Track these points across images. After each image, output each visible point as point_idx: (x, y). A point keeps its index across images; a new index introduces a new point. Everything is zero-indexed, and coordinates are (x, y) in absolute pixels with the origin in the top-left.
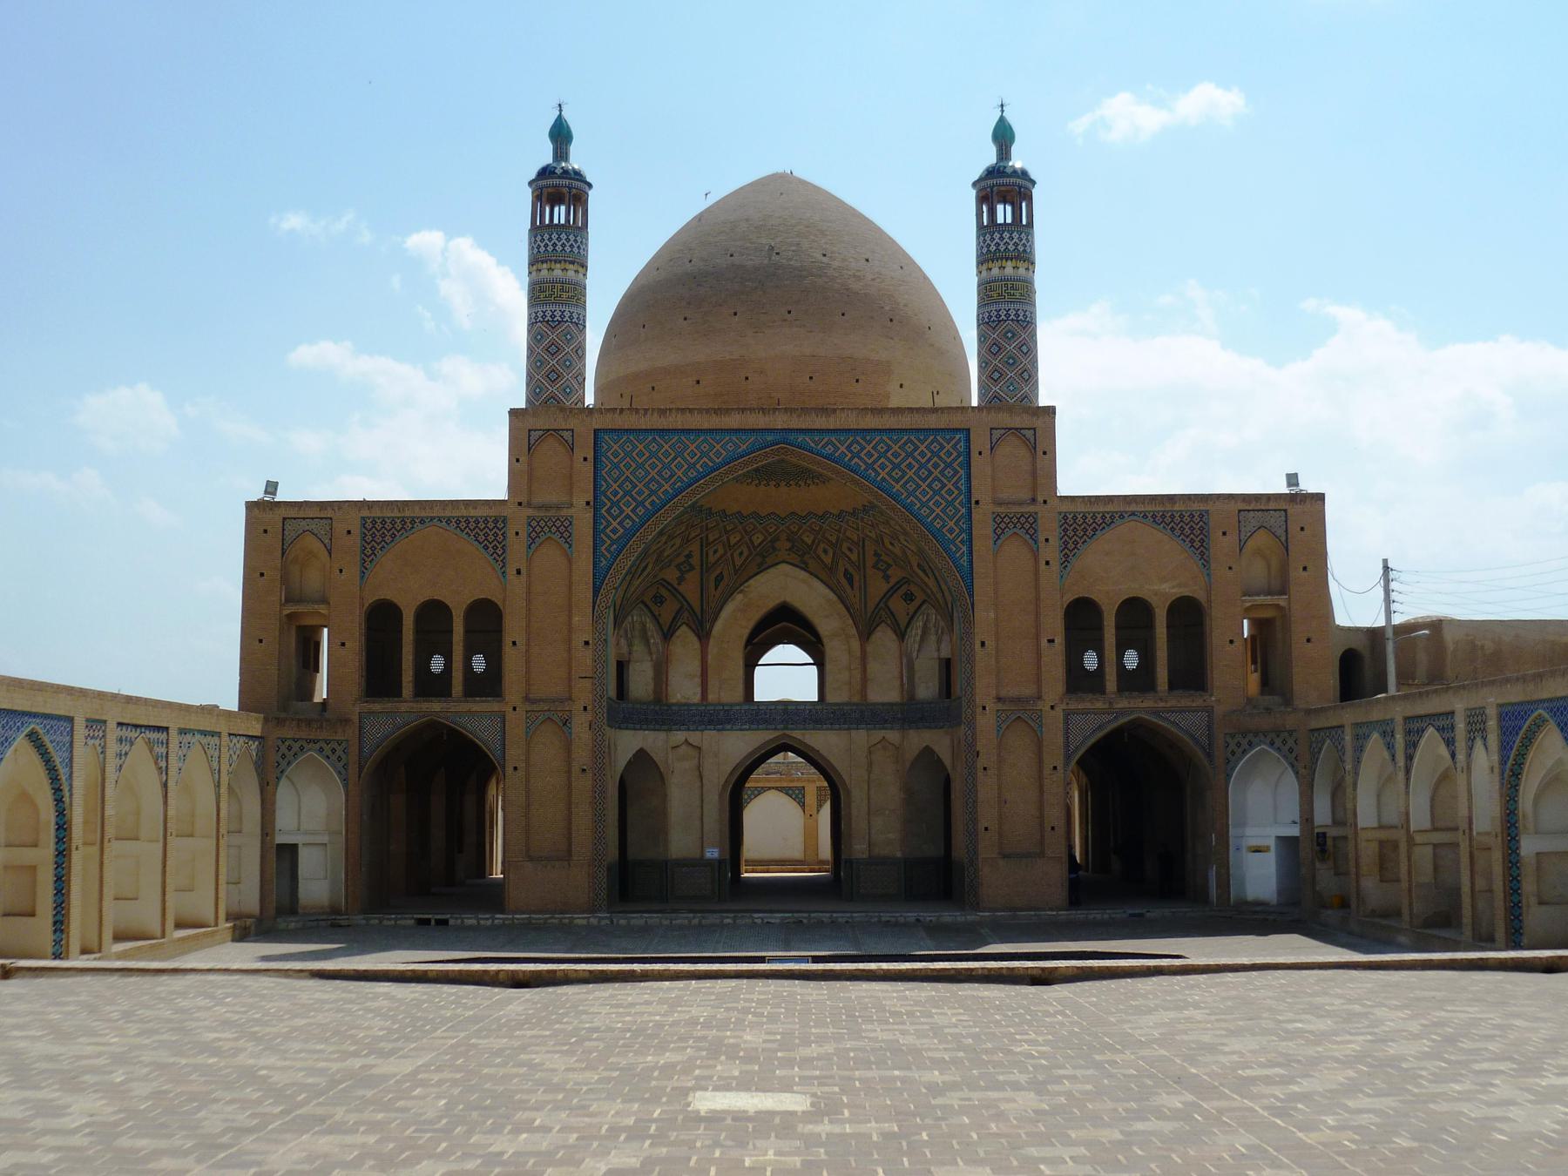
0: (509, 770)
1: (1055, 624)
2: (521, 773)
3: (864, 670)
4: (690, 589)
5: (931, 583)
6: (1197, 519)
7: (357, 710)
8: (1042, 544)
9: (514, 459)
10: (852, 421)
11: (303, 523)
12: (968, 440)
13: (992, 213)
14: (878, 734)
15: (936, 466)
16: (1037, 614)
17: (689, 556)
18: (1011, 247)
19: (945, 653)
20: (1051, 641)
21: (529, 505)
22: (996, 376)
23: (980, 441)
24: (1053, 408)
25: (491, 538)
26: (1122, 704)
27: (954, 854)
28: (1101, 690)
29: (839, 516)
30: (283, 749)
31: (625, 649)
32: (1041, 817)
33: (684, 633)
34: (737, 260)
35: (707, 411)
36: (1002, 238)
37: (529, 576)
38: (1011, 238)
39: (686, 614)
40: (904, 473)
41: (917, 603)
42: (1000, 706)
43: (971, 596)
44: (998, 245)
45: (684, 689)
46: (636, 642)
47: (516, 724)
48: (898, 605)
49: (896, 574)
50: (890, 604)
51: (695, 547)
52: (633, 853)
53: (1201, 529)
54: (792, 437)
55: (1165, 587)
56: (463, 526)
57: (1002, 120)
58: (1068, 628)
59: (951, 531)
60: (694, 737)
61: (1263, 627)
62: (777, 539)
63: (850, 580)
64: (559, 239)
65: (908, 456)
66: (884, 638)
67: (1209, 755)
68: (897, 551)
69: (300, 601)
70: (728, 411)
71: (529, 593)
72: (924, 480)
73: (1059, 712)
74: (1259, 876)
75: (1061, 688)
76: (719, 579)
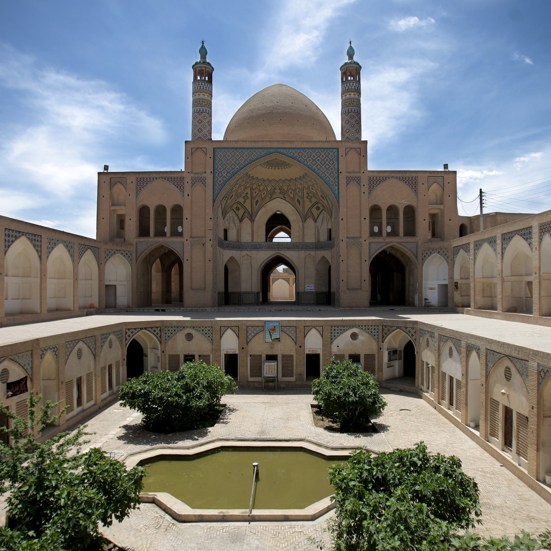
0: (185, 260)
1: (366, 213)
2: (189, 261)
3: (304, 232)
4: (248, 205)
5: (325, 202)
6: (414, 179)
7: (135, 241)
8: (362, 186)
9: (187, 158)
10: (299, 145)
11: (117, 179)
12: (338, 152)
13: (347, 79)
14: (308, 252)
15: (327, 160)
16: (360, 211)
17: (247, 194)
18: (353, 88)
19: (329, 227)
20: (365, 219)
21: (192, 173)
22: (348, 131)
23: (342, 152)
24: (367, 141)
25: (179, 184)
26: (388, 240)
27: (332, 290)
28: (382, 236)
29: (295, 180)
30: (107, 252)
31: (228, 225)
32: (361, 277)
33: (246, 221)
34: (264, 104)
35: (251, 141)
36: (350, 85)
37: (192, 196)
38: (353, 85)
39: (247, 214)
40: (317, 163)
41: (320, 210)
42: (348, 240)
43: (339, 203)
44: (348, 87)
45: (246, 238)
46: (231, 223)
47: (187, 245)
48: (314, 210)
49: (314, 200)
50: (312, 210)
51: (248, 190)
52: (230, 290)
53: (415, 182)
54: (279, 150)
55: (403, 201)
56: (170, 179)
57: (351, 46)
58: (371, 215)
59: (332, 182)
60: (249, 253)
61: (433, 217)
62: (275, 189)
63: (299, 204)
64: (202, 85)
65: (318, 157)
66: (310, 221)
67: (416, 257)
68: (314, 191)
69: (118, 205)
70: (258, 141)
71: (192, 202)
72: (323, 165)
73: (367, 242)
74: (433, 296)
75: (368, 234)
76: (257, 202)
